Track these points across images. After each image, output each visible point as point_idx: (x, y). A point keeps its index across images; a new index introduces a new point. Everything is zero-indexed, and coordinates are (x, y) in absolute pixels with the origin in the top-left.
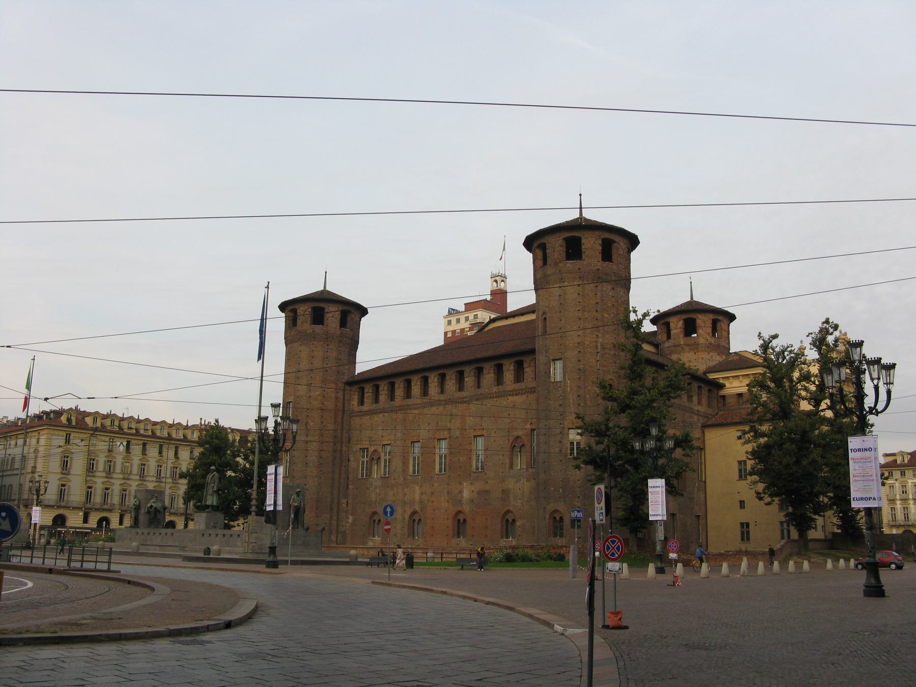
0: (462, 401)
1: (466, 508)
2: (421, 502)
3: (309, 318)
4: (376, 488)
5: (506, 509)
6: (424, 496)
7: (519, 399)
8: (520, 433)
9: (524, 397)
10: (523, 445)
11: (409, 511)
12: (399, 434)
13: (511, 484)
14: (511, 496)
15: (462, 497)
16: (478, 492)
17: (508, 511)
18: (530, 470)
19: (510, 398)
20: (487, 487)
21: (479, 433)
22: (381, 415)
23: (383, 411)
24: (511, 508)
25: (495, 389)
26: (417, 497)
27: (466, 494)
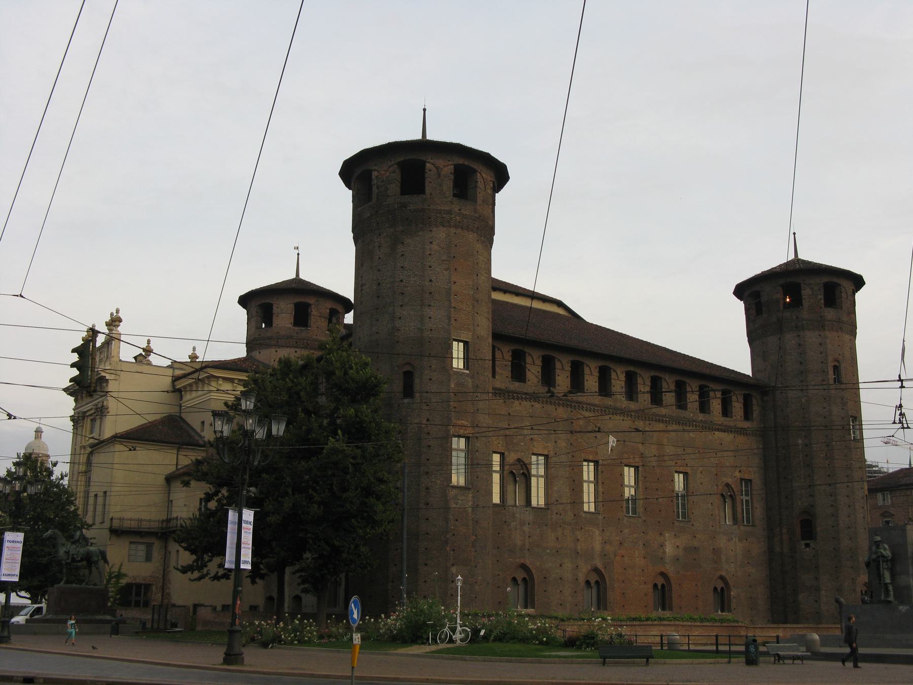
0: (660, 419)
1: (670, 570)
2: (604, 555)
3: (448, 185)
4: (522, 524)
5: (719, 574)
6: (608, 547)
7: (727, 437)
8: (730, 481)
9: (732, 436)
10: (731, 496)
11: (584, 568)
12: (562, 444)
13: (722, 542)
14: (724, 558)
15: (664, 552)
16: (685, 549)
17: (722, 578)
18: (742, 527)
19: (716, 433)
20: (696, 543)
21: (682, 469)
22: (526, 404)
23: (533, 397)
24: (724, 574)
25: (701, 417)
26: (598, 547)
27: (669, 550)
